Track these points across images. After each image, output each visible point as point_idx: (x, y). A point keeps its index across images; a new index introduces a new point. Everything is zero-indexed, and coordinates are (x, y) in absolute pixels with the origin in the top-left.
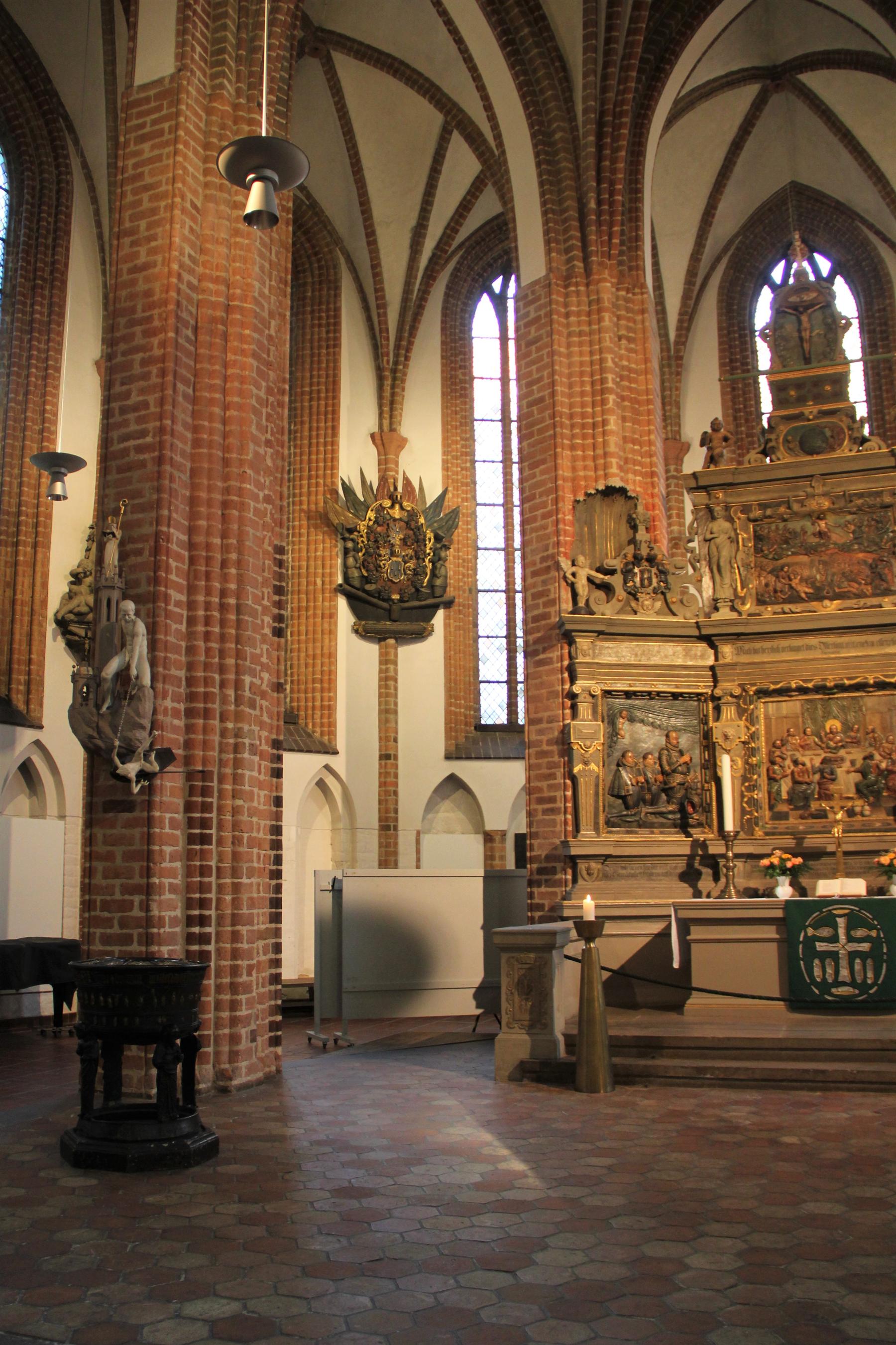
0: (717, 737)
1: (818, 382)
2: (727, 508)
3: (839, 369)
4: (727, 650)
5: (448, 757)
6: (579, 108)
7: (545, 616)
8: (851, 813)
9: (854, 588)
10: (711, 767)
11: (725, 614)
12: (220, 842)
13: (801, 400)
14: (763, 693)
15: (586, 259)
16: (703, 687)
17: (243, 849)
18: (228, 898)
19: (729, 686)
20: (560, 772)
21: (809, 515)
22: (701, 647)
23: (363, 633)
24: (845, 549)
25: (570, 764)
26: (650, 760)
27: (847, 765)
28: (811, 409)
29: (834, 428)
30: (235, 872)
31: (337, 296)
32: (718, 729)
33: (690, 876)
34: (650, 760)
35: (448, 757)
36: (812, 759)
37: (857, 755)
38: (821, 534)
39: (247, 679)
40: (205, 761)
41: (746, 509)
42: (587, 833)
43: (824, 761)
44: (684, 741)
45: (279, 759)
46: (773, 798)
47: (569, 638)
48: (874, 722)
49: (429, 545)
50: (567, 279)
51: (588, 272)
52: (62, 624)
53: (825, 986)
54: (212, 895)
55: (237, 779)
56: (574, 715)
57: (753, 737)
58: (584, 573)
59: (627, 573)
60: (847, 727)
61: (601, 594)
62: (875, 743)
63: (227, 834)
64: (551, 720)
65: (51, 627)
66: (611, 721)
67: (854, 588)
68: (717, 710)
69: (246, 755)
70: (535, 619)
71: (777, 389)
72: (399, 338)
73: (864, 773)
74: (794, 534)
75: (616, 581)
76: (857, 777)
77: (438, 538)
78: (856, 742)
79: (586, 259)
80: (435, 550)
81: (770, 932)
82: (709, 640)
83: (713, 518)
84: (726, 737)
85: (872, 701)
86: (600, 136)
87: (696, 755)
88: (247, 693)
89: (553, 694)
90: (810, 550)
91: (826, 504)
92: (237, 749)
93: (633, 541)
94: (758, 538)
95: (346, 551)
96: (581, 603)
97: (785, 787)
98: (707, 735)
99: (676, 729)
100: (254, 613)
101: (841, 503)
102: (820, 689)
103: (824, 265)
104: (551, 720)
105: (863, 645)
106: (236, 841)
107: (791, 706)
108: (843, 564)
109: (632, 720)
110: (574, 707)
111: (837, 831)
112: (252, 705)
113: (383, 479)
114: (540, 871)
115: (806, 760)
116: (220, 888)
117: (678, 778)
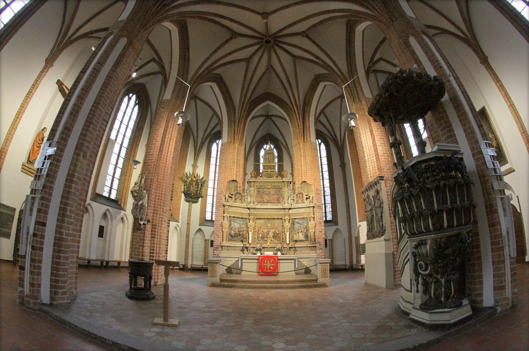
0: (249, 226)
1: (271, 166)
2: (254, 185)
3: (274, 164)
5: (199, 225)
7: (220, 202)
8: (271, 240)
9: (274, 201)
11: (252, 204)
12: (157, 238)
13: (268, 169)
14: (257, 219)
15: (234, 140)
16: (247, 217)
17: (161, 240)
18: (158, 249)
19: (251, 217)
20: (220, 230)
21: (268, 188)
22: (248, 209)
23: (187, 201)
24: (273, 195)
25: (222, 229)
26: (237, 229)
27: (271, 232)
28: (269, 170)
29: (273, 174)
30: (160, 245)
31: (190, 139)
32: (249, 224)
33: (242, 250)
34: (237, 229)
35: (199, 225)
36: (265, 231)
37: (273, 230)
38: (269, 192)
39: (165, 208)
40: (156, 223)
41: (257, 186)
42: (225, 241)
43: (267, 231)
44: (243, 226)
45: (169, 223)
46: (258, 237)
48: (276, 225)
49: (200, 186)
51: (234, 142)
52: (132, 192)
54: (155, 248)
55: (161, 227)
56: (224, 220)
57: (255, 226)
59: (235, 195)
60: (271, 226)
61: (230, 199)
63: (159, 237)
64: (219, 221)
65: (130, 192)
66: (230, 222)
67: (274, 201)
68: (249, 221)
69: (163, 222)
70: (218, 202)
71: (264, 166)
72: (199, 148)
73: (274, 234)
74: (265, 191)
75: (233, 196)
76: (273, 234)
77: (201, 185)
78: (273, 228)
79: (234, 140)
80: (201, 187)
81: (256, 261)
82: (249, 208)
83: (251, 187)
84: (251, 226)
85: (276, 221)
87: (245, 229)
88: (165, 211)
89: (220, 216)
90: (268, 194)
91: (271, 187)
92: (162, 221)
93: (237, 190)
94: (259, 191)
95: (185, 185)
96: (227, 200)
97: (260, 235)
98: (247, 225)
99: (242, 224)
100: (167, 195)
101: (273, 187)
102: (267, 219)
103: (272, 147)
104: (219, 221)
105: (275, 211)
106: (160, 238)
107: (262, 221)
108: (272, 197)
109: (234, 222)
110: (224, 219)
111: (268, 244)
112: (165, 213)
113: (193, 173)
114: (216, 248)
115: (264, 231)
116: (157, 247)
117: (241, 233)
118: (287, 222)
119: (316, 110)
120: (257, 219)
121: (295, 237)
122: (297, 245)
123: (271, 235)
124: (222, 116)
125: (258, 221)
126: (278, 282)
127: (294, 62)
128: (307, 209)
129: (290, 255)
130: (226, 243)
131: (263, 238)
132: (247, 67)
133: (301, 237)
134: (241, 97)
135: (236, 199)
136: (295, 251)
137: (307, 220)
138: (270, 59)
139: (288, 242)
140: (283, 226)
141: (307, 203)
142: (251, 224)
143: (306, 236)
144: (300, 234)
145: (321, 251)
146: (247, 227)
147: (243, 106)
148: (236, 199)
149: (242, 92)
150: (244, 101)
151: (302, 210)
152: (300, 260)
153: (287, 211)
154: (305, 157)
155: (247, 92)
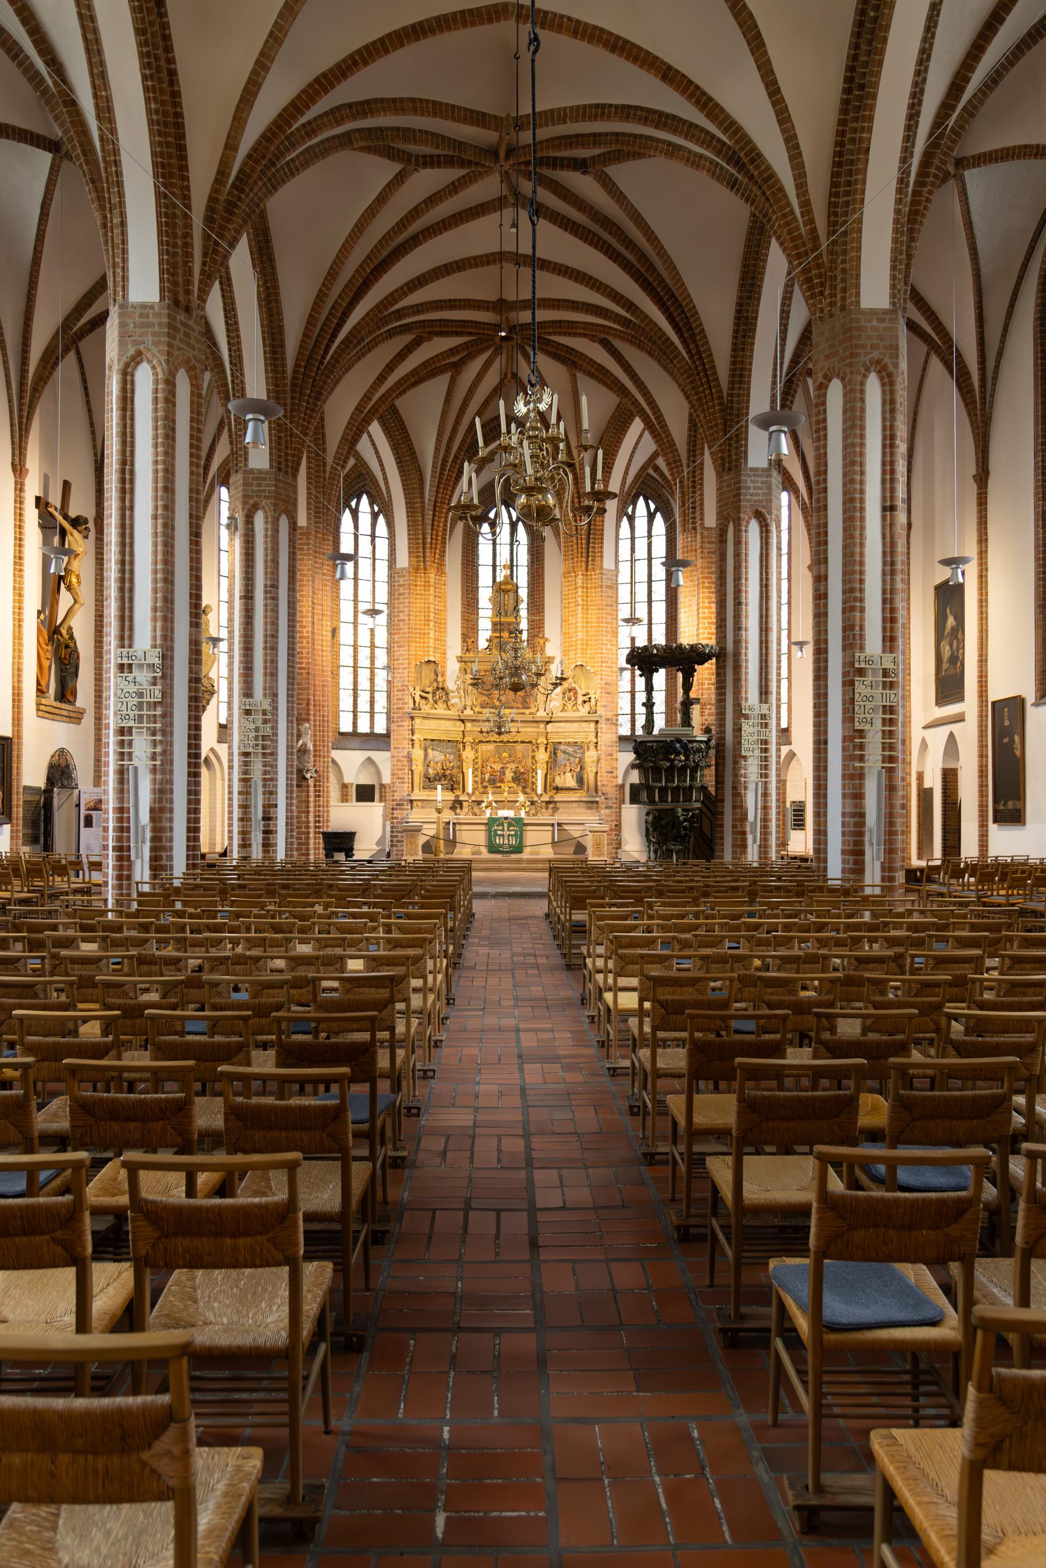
0: (464, 757)
4: (469, 725)
6: (427, 497)
10: (460, 767)
15: (424, 562)
16: (459, 738)
33: (453, 808)
36: (497, 767)
37: (513, 766)
46: (483, 780)
47: (412, 718)
50: (417, 569)
51: (425, 569)
53: (500, 846)
58: (418, 693)
59: (434, 693)
62: (520, 762)
66: (426, 750)
75: (430, 696)
79: (424, 562)
81: (483, 827)
82: (463, 721)
86: (434, 510)
87: (455, 763)
93: (436, 680)
97: (487, 776)
98: (460, 756)
118: (542, 749)
119: (626, 472)
120: (481, 742)
121: (559, 781)
122: (559, 797)
123: (509, 775)
124: (385, 479)
125: (483, 747)
126: (520, 861)
127: (574, 377)
128: (584, 725)
129: (545, 817)
130: (418, 794)
131: (492, 782)
132: (453, 381)
133: (570, 781)
134: (437, 450)
135: (436, 702)
136: (555, 809)
137: (582, 747)
138: (511, 360)
139: (539, 791)
140: (533, 757)
141: (583, 711)
142: (468, 754)
143: (580, 780)
144: (568, 775)
145: (607, 811)
146: (461, 760)
147: (441, 473)
148: (436, 702)
149: (439, 440)
150: (445, 460)
151: (575, 726)
152: (566, 827)
153: (542, 726)
154: (586, 608)
155: (451, 439)
